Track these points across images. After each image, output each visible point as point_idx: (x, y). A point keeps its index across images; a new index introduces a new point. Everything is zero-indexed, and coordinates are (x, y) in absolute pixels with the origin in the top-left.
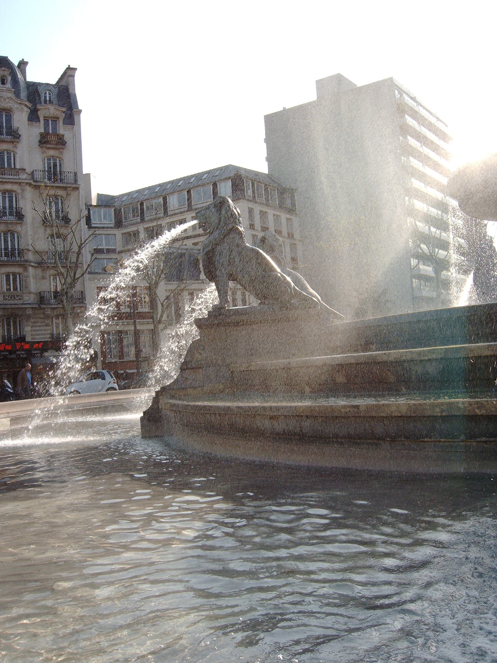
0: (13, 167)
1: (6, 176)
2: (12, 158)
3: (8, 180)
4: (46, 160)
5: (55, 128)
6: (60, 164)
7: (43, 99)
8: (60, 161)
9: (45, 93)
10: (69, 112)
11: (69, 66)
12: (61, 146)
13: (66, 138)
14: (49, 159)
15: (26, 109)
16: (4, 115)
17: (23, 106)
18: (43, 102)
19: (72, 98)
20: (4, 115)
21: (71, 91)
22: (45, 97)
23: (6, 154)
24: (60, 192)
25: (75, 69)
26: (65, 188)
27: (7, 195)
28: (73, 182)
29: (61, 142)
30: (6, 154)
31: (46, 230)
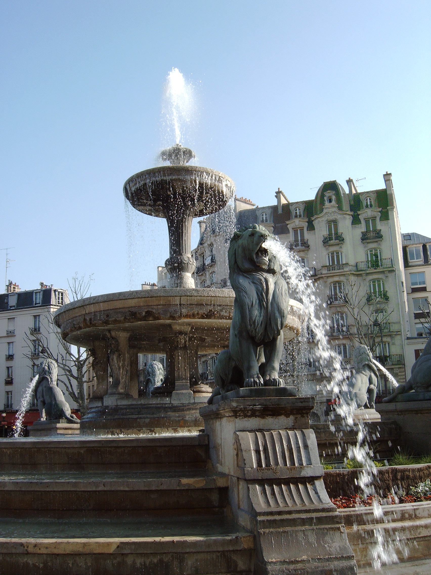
0: (341, 263)
1: (336, 271)
2: (340, 255)
3: (334, 274)
4: (369, 252)
5: (374, 225)
6: (380, 252)
7: (364, 204)
8: (380, 250)
9: (367, 200)
10: (386, 210)
11: (387, 172)
12: (379, 239)
13: (382, 233)
14: (371, 251)
15: (348, 217)
16: (333, 225)
17: (345, 215)
18: (364, 207)
19: (389, 197)
20: (333, 225)
21: (388, 192)
22: (367, 202)
23: (335, 254)
24: (380, 276)
25: (390, 174)
26: (383, 272)
27: (337, 285)
28: (391, 266)
29: (379, 236)
30: (335, 254)
31: (370, 308)
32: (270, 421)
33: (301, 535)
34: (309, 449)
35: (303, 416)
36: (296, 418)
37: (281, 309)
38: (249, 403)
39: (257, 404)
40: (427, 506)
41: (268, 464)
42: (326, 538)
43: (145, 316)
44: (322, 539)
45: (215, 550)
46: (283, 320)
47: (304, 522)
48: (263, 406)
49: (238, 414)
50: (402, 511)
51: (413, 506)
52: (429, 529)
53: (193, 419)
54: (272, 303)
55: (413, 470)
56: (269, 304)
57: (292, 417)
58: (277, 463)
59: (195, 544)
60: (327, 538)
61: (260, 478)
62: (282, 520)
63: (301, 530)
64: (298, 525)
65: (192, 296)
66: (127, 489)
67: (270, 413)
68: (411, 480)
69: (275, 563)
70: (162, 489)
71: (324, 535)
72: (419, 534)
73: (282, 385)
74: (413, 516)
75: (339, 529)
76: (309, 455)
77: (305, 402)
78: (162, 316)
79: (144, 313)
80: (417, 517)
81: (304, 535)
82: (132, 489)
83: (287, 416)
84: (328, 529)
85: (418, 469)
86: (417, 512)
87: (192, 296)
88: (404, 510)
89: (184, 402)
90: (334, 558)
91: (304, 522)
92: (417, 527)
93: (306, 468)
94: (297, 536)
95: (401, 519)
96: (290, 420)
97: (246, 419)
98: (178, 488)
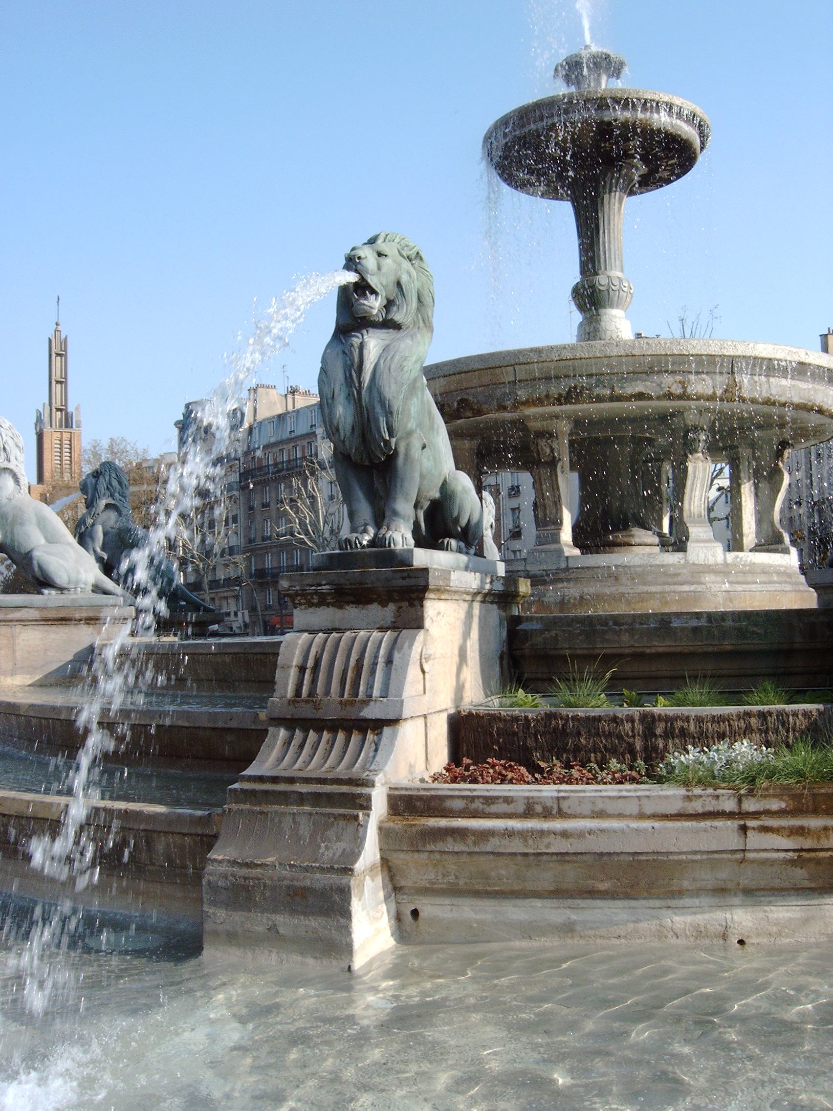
32: (352, 612)
33: (288, 822)
34: (394, 667)
35: (412, 605)
36: (400, 608)
37: (385, 398)
38: (307, 582)
39: (324, 582)
40: (593, 794)
41: (312, 693)
42: (328, 833)
43: (458, 410)
44: (323, 834)
45: (178, 831)
46: (390, 419)
47: (301, 799)
48: (334, 587)
49: (297, 602)
50: (528, 798)
51: (559, 791)
52: (570, 840)
53: (559, 599)
54: (370, 388)
55: (699, 720)
56: (363, 392)
57: (392, 607)
58: (327, 692)
59: (152, 818)
60: (330, 833)
61: (289, 717)
62: (266, 792)
63: (290, 813)
64: (292, 804)
65: (528, 363)
66: (186, 724)
67: (351, 598)
68: (694, 738)
69: (220, 862)
70: (232, 726)
71: (328, 826)
72: (548, 846)
73: (399, 547)
74: (554, 812)
75: (356, 818)
76: (389, 679)
77: (409, 577)
78: (485, 407)
79: (456, 404)
80: (562, 814)
81: (294, 822)
82: (192, 725)
83: (384, 604)
84: (337, 817)
85: (714, 717)
86: (564, 805)
87: (528, 363)
88: (533, 797)
89: (549, 568)
90: (318, 868)
91: (301, 799)
92: (542, 833)
93: (372, 703)
94: (280, 822)
95: (525, 813)
96: (388, 612)
97: (311, 610)
98: (253, 727)
